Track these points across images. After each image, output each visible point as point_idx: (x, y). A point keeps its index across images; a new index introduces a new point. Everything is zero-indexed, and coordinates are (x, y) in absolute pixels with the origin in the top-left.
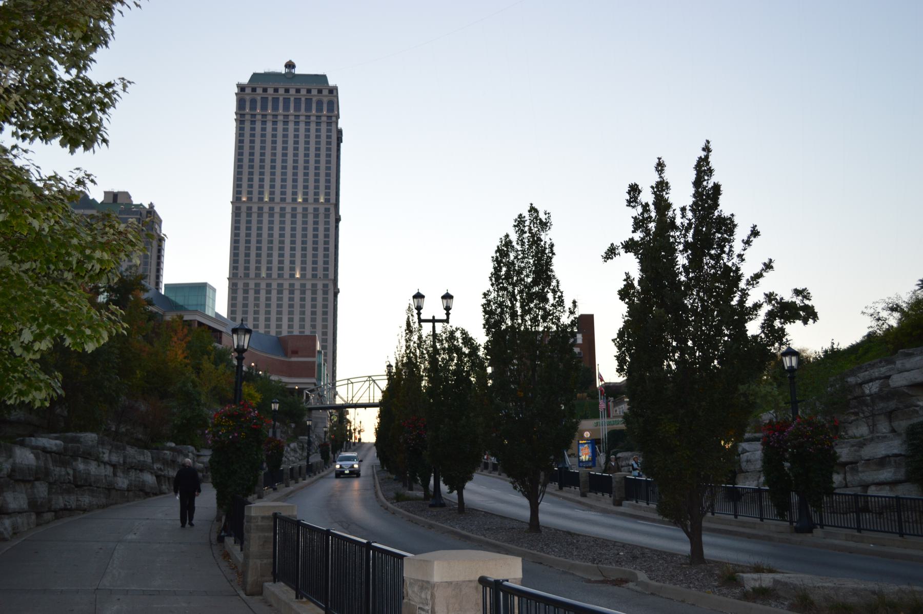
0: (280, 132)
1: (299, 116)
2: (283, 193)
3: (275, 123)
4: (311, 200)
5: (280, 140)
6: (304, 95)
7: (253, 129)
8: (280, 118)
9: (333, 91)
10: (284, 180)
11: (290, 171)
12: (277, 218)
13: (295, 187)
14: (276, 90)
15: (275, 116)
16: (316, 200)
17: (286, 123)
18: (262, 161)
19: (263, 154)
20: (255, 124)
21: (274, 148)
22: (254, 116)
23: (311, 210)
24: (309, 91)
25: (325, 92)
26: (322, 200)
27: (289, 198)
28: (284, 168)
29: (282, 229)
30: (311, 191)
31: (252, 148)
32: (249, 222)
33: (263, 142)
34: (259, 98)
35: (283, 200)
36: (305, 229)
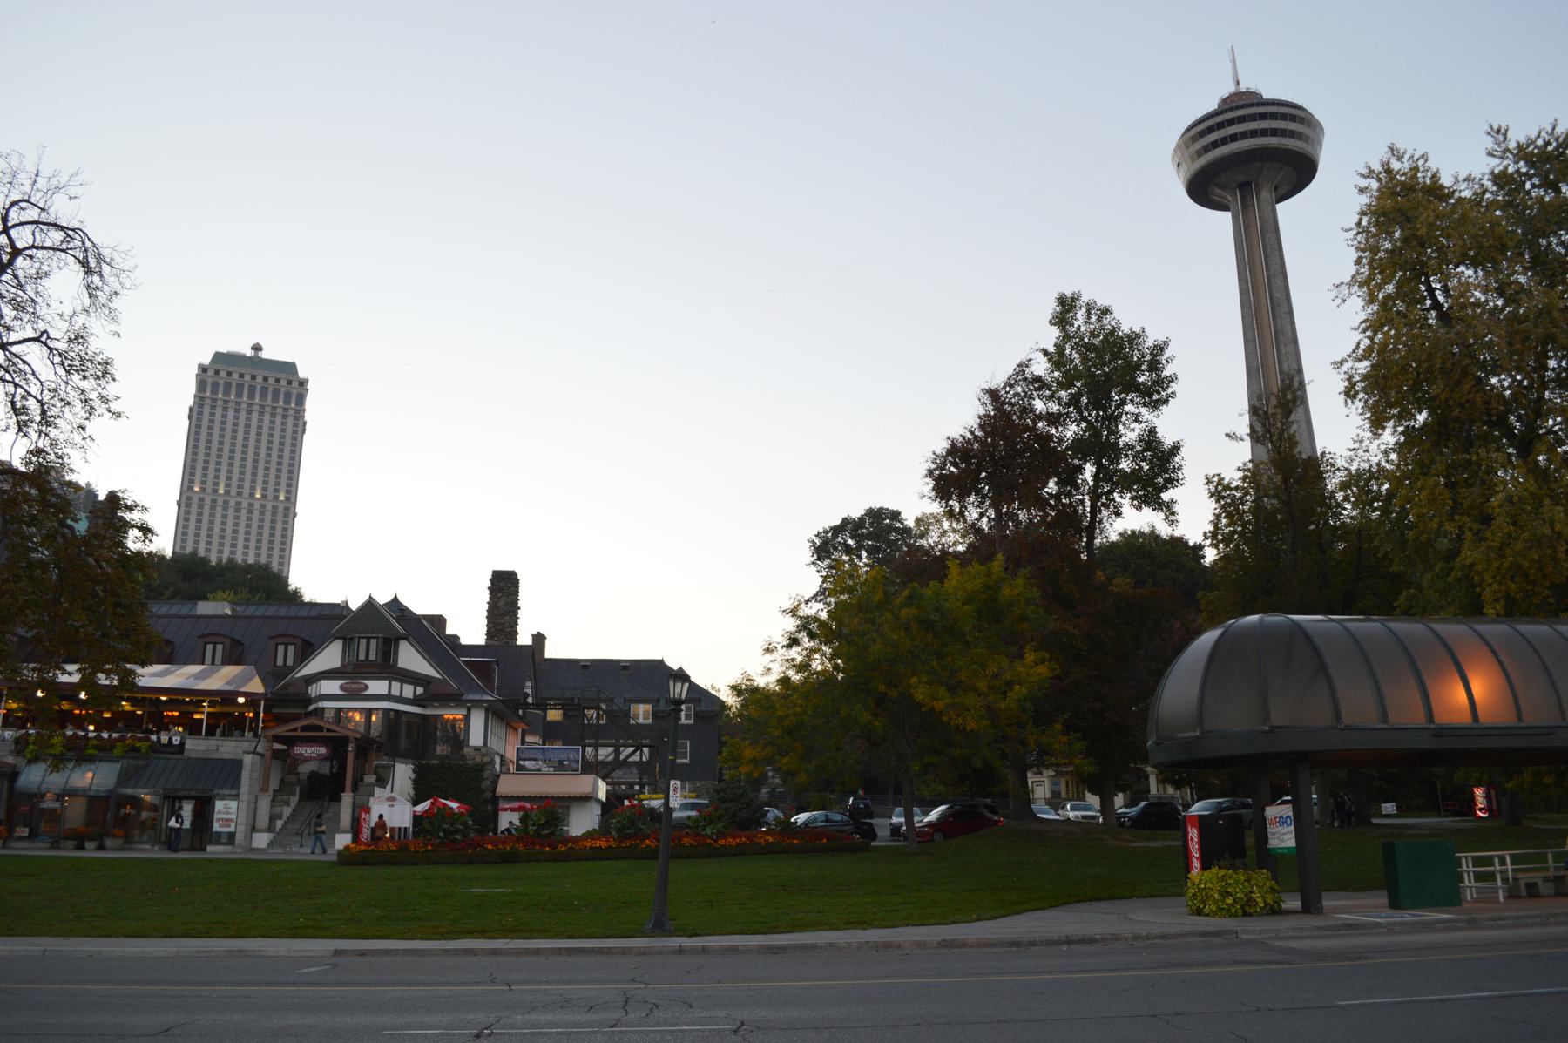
0: (242, 421)
2: (240, 487)
4: (270, 497)
7: (212, 415)
8: (244, 406)
9: (303, 383)
10: (243, 473)
12: (231, 512)
14: (241, 376)
15: (238, 403)
16: (276, 498)
17: (249, 412)
18: (220, 450)
19: (221, 443)
20: (215, 409)
21: (234, 438)
22: (214, 400)
24: (277, 381)
25: (295, 384)
26: (282, 498)
27: (246, 492)
28: (244, 459)
29: (236, 525)
30: (271, 487)
31: (210, 435)
32: (200, 514)
33: (223, 429)
34: (222, 382)
35: (239, 494)
36: (260, 527)
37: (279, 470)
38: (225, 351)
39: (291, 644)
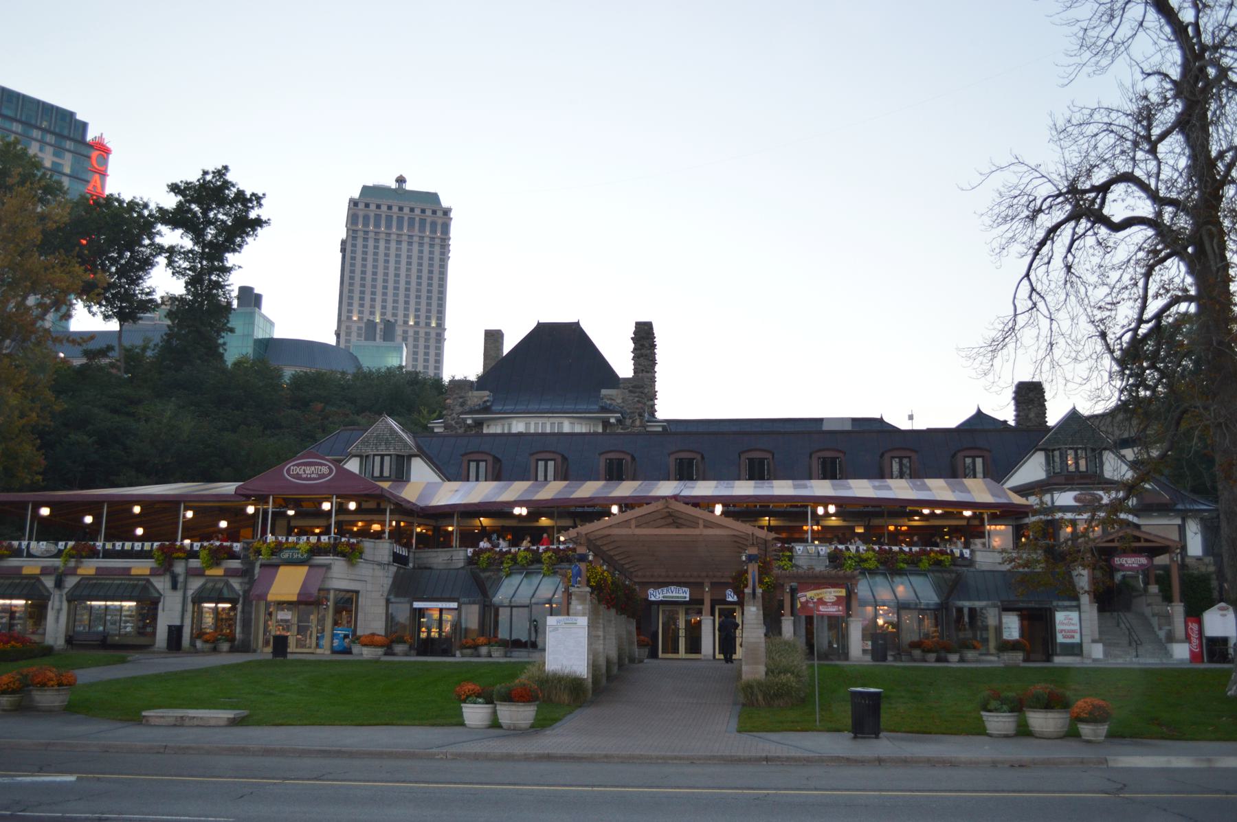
0: (393, 252)
1: (412, 236)
3: (388, 241)
4: (422, 324)
6: (418, 215)
7: (365, 246)
8: (394, 237)
11: (402, 292)
13: (406, 309)
14: (390, 208)
15: (389, 234)
18: (374, 280)
19: (375, 273)
21: (386, 268)
22: (366, 233)
23: (422, 334)
24: (423, 211)
25: (440, 214)
26: (433, 325)
28: (396, 288)
30: (423, 313)
31: (364, 266)
33: (376, 260)
34: (372, 215)
37: (429, 298)
38: (371, 185)
39: (551, 460)
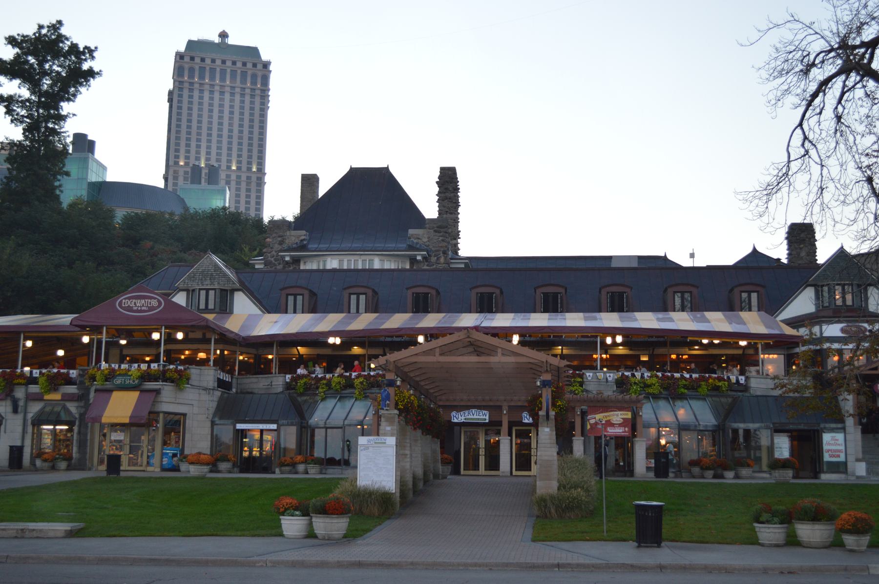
0: (216, 102)
3: (212, 92)
4: (244, 168)
5: (216, 110)
6: (240, 68)
8: (217, 88)
9: (266, 65)
10: (219, 148)
11: (225, 140)
13: (229, 155)
15: (212, 86)
16: (249, 169)
17: (222, 93)
18: (199, 128)
19: (200, 122)
20: (193, 92)
21: (210, 117)
22: (191, 84)
23: (244, 178)
25: (260, 66)
28: (220, 136)
30: (244, 159)
31: (190, 115)
33: (200, 110)
34: (197, 67)
37: (250, 145)
38: (196, 39)
